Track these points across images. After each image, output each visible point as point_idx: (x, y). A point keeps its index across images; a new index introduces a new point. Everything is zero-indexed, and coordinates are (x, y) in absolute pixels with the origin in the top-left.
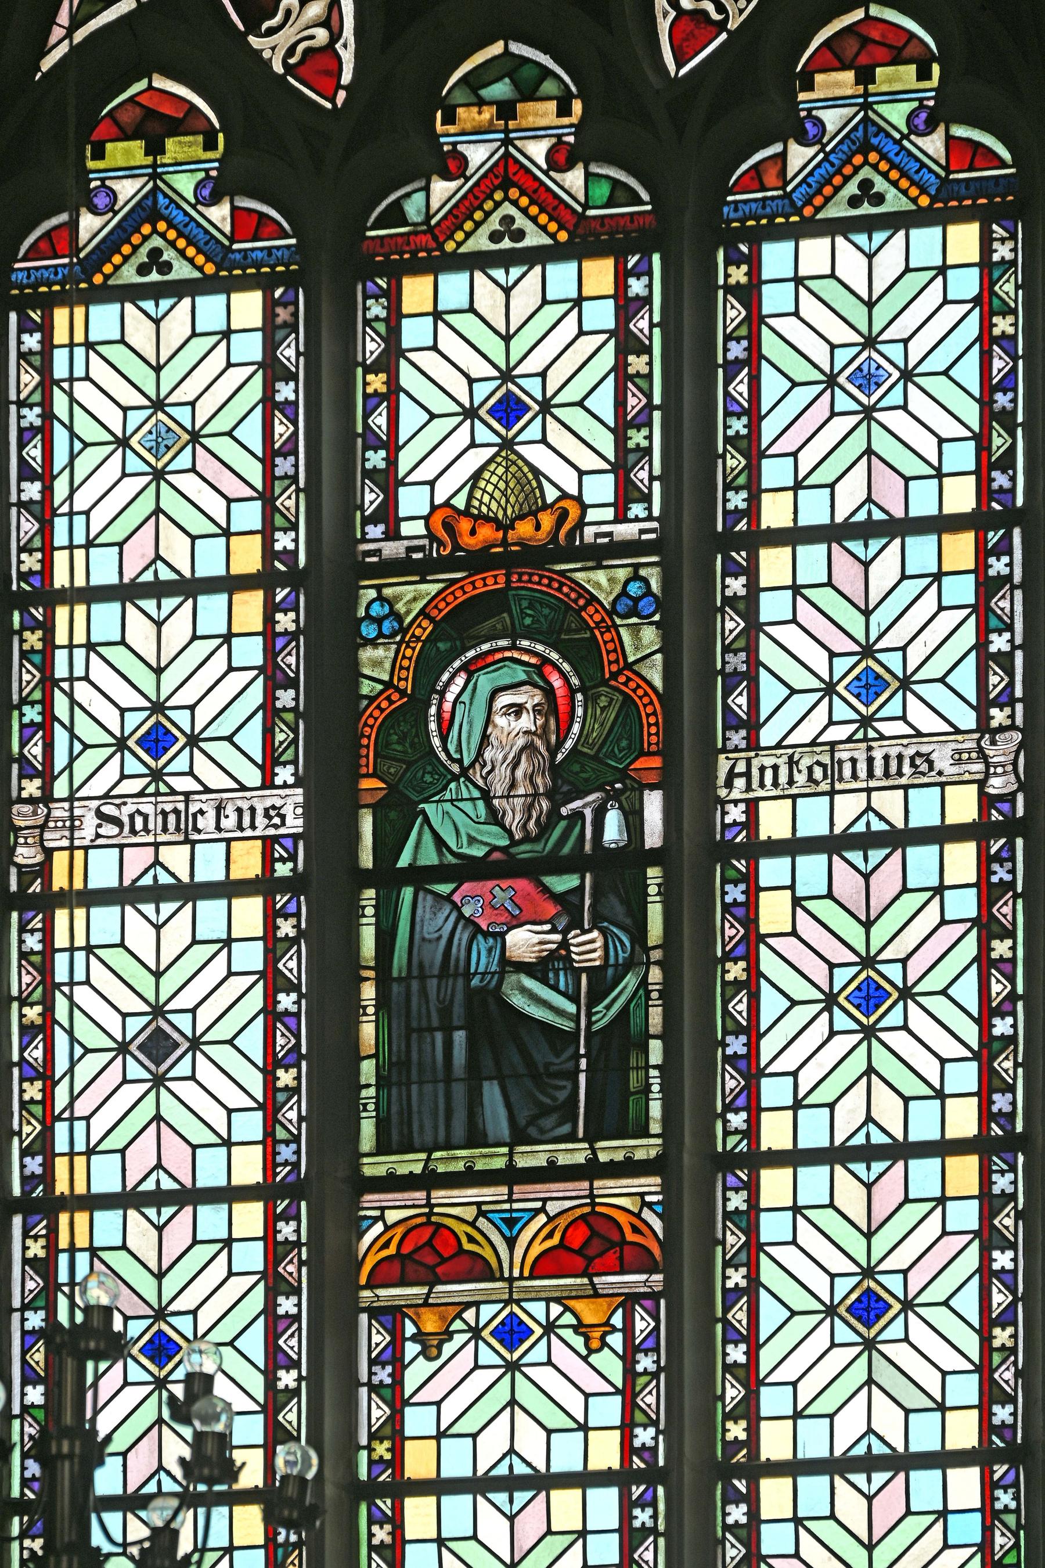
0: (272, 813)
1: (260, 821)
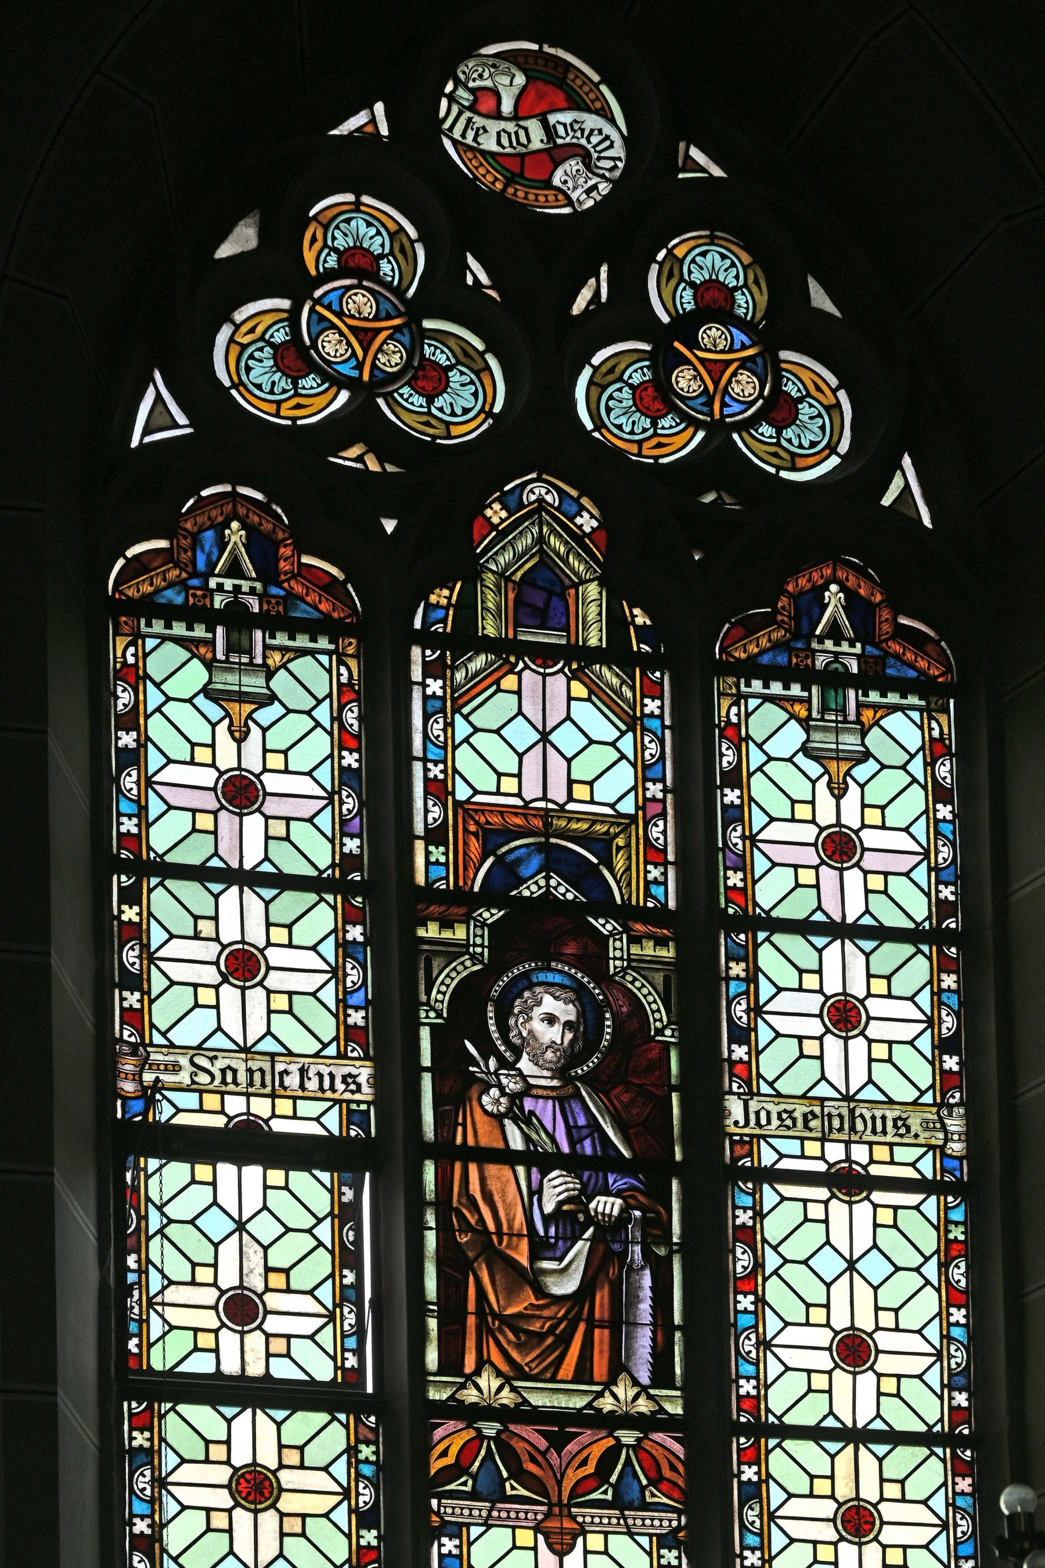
1: (340, 1086)
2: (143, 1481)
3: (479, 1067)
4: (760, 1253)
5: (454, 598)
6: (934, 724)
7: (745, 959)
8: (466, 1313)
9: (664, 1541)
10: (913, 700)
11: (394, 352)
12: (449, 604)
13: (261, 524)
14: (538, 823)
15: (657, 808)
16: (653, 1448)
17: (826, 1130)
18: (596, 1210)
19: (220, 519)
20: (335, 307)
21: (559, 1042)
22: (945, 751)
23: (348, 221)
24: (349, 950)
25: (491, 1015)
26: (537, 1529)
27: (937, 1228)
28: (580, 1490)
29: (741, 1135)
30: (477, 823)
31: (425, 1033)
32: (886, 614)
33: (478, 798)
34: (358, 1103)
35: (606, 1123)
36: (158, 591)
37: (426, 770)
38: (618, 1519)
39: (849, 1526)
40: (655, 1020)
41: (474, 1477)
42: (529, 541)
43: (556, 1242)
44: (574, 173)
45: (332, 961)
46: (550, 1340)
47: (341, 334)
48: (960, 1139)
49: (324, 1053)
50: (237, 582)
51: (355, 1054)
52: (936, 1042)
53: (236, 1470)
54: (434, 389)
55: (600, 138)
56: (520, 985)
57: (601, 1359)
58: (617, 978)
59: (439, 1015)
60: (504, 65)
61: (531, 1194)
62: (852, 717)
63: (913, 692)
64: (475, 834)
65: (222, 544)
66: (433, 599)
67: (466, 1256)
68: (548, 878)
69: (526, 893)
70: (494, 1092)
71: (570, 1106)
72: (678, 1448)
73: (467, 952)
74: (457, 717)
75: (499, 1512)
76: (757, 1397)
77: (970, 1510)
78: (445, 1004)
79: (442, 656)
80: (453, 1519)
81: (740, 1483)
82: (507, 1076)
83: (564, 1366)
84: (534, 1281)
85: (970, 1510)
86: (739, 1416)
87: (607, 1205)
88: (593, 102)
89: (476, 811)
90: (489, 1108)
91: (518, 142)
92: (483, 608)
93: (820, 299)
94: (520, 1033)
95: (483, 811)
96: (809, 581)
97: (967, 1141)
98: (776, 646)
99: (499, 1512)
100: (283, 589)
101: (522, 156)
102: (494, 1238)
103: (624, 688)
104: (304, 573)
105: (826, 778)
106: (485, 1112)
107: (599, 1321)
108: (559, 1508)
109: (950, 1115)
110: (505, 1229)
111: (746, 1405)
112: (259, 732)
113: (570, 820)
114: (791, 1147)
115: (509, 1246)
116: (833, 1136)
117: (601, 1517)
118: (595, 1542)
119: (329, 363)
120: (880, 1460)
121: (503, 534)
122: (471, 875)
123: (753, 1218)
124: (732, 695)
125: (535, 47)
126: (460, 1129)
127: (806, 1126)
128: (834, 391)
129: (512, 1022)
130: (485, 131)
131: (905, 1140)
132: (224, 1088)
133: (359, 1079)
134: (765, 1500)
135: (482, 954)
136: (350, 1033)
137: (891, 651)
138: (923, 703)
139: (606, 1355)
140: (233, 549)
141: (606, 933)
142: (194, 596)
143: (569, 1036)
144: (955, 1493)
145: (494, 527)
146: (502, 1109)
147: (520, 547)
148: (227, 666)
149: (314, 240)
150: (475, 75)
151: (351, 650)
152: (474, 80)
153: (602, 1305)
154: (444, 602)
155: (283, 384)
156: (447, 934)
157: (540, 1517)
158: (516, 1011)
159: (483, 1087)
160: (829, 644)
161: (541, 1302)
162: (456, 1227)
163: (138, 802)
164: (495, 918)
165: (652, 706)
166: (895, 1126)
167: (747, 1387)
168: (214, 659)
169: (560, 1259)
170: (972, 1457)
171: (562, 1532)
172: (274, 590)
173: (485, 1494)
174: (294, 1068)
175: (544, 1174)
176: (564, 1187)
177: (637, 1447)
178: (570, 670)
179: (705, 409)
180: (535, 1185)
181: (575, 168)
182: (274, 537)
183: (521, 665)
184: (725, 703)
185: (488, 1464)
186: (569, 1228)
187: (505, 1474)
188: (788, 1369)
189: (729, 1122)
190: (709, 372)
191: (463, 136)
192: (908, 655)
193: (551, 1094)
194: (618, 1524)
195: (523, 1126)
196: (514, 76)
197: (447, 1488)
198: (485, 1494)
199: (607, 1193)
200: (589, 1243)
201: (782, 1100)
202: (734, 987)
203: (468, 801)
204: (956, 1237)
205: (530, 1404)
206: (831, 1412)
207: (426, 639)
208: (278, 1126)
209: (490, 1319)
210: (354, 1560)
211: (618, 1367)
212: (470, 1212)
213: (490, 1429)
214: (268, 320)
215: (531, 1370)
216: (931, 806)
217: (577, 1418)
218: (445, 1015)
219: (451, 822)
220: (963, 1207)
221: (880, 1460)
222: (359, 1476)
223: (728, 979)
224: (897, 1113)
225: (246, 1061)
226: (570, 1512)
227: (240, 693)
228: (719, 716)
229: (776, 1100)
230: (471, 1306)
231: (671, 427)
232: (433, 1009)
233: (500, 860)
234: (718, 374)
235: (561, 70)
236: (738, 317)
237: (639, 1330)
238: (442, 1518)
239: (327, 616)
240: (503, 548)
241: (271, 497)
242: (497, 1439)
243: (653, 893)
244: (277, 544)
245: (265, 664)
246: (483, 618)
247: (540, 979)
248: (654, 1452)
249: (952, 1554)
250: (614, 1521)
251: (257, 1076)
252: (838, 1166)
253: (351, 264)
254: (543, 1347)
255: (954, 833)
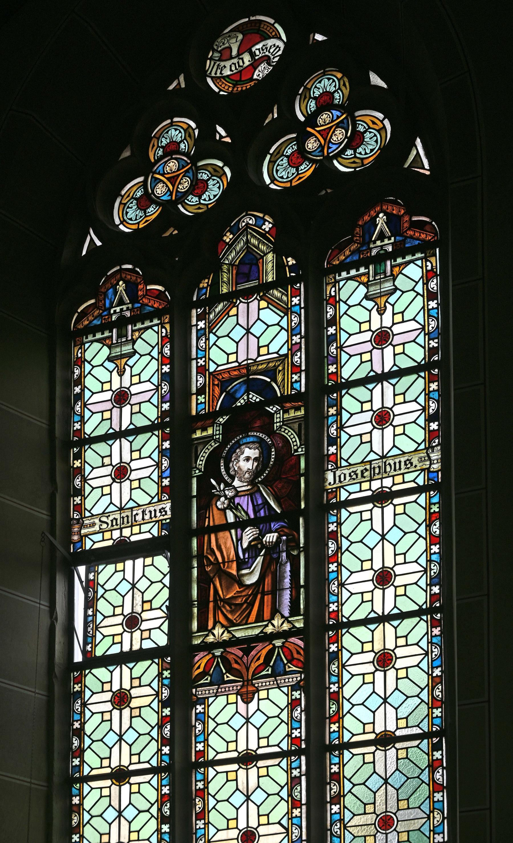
0: (162, 511)
1: (158, 514)
2: (77, 706)
3: (216, 489)
4: (339, 542)
5: (210, 282)
6: (428, 264)
7: (336, 405)
8: (209, 602)
9: (294, 688)
10: (419, 255)
11: (185, 182)
12: (208, 285)
13: (131, 278)
14: (244, 371)
15: (297, 347)
16: (289, 645)
17: (372, 475)
18: (266, 541)
19: (115, 282)
20: (161, 172)
21: (251, 468)
22: (434, 274)
23: (167, 132)
24: (164, 453)
25: (222, 464)
26: (237, 694)
27: (425, 509)
28: (256, 672)
29: (332, 489)
30: (218, 380)
31: (194, 481)
32: (406, 218)
33: (220, 368)
34: (166, 519)
35: (270, 499)
36: (91, 322)
37: (197, 363)
38: (273, 681)
39: (380, 663)
40: (294, 446)
41: (211, 676)
42: (242, 244)
43: (248, 560)
44: (263, 69)
45: (157, 460)
46: (245, 606)
47: (164, 183)
48: (437, 462)
49: (153, 501)
50: (121, 307)
51: (165, 498)
52: (427, 418)
53: (114, 693)
54: (202, 191)
55: (275, 48)
56: (235, 448)
57: (267, 609)
58: (277, 432)
59: (200, 471)
60: (233, 34)
61: (237, 541)
62: (389, 274)
63: (417, 252)
64: (217, 385)
65: (115, 292)
66: (201, 285)
67: (210, 576)
68: (248, 396)
69: (239, 404)
70: (222, 499)
71: (255, 496)
72: (301, 643)
73: (213, 439)
74: (211, 335)
75: (221, 689)
76: (338, 611)
77: (439, 643)
78: (203, 465)
79: (205, 309)
80: (202, 696)
81: (329, 653)
82: (228, 490)
83: (251, 616)
84: (238, 580)
85: (439, 643)
86: (329, 621)
87: (271, 537)
88: (271, 33)
89: (218, 374)
90: (220, 507)
91: (239, 66)
92: (222, 282)
93: (375, 80)
94: (234, 469)
95: (221, 374)
96: (369, 216)
97: (441, 462)
98: (353, 253)
99: (221, 689)
100: (140, 303)
101: (240, 72)
102: (222, 565)
103: (283, 296)
104: (148, 294)
105: (376, 306)
106: (218, 509)
107: (267, 592)
108: (247, 683)
109: (433, 451)
110: (226, 560)
111: (333, 616)
112: (129, 368)
113: (258, 365)
114: (356, 487)
115: (228, 567)
116: (375, 478)
117: (266, 682)
118: (263, 694)
119: (158, 198)
120: (396, 628)
121: (231, 246)
122: (215, 404)
123: (337, 527)
124: (332, 283)
125: (247, 20)
126: (207, 519)
127: (363, 476)
128: (382, 121)
129: (231, 465)
130: (225, 67)
131: (410, 470)
132: (112, 528)
133: (166, 509)
134: (340, 659)
135: (219, 438)
136: (163, 490)
137: (408, 235)
138: (423, 255)
139: (270, 607)
140: (120, 293)
141: (273, 412)
142: (105, 319)
143: (256, 464)
144: (432, 636)
145: (227, 244)
146: (225, 506)
147: (238, 249)
148: (120, 345)
149: (154, 146)
150: (221, 44)
151: (167, 320)
152: (221, 47)
153: (268, 584)
154: (206, 285)
155: (140, 214)
156: (205, 434)
157: (239, 688)
158: (233, 460)
159: (217, 498)
160: (379, 243)
161: (241, 589)
162: (206, 564)
163: (80, 415)
164: (225, 420)
165: (295, 300)
166: (406, 464)
167: (333, 607)
168: (112, 344)
169: (250, 568)
170: (441, 617)
171: (247, 693)
172: (137, 305)
173: (215, 682)
174: (140, 512)
175: (243, 531)
176: (252, 534)
177: (282, 647)
178: (260, 297)
179: (320, 154)
180: (239, 537)
181: (263, 67)
182: (136, 282)
183: (238, 301)
184: (329, 288)
185: (217, 668)
186: (254, 552)
187: (224, 671)
188: (352, 594)
189: (327, 484)
190: (322, 136)
191: (216, 74)
192: (416, 234)
193: (247, 493)
194: (274, 684)
195: (234, 511)
196: (238, 37)
197: (199, 683)
198: (215, 682)
199: (271, 532)
200: (263, 557)
201: (352, 467)
202: (331, 420)
203: (215, 371)
204: (434, 511)
205: (236, 637)
206: (373, 610)
207: (198, 304)
208: (133, 539)
209: (219, 602)
210: (160, 723)
211: (275, 611)
212: (211, 556)
213: (218, 652)
214: (135, 188)
215: (237, 621)
216: (426, 304)
217: (257, 639)
218: (203, 470)
219: (207, 383)
220: (438, 495)
221: (396, 628)
222: (163, 685)
223: (328, 416)
224: (406, 458)
225: (120, 514)
226: (252, 682)
227: (121, 355)
228: (326, 295)
229: (348, 468)
230: (211, 598)
231: (305, 168)
232: (198, 469)
233: (228, 393)
234: (326, 135)
235: (258, 25)
236: (336, 105)
237: (285, 592)
238: (197, 697)
239: (157, 309)
240: (231, 252)
241: (135, 266)
242: (221, 657)
243: (295, 387)
244: (138, 284)
245: (132, 339)
246: (222, 286)
247: (244, 442)
248: (290, 647)
249: (430, 666)
250: (272, 683)
251: (125, 519)
252: (377, 491)
253: (168, 150)
254: (242, 610)
255: (438, 313)
